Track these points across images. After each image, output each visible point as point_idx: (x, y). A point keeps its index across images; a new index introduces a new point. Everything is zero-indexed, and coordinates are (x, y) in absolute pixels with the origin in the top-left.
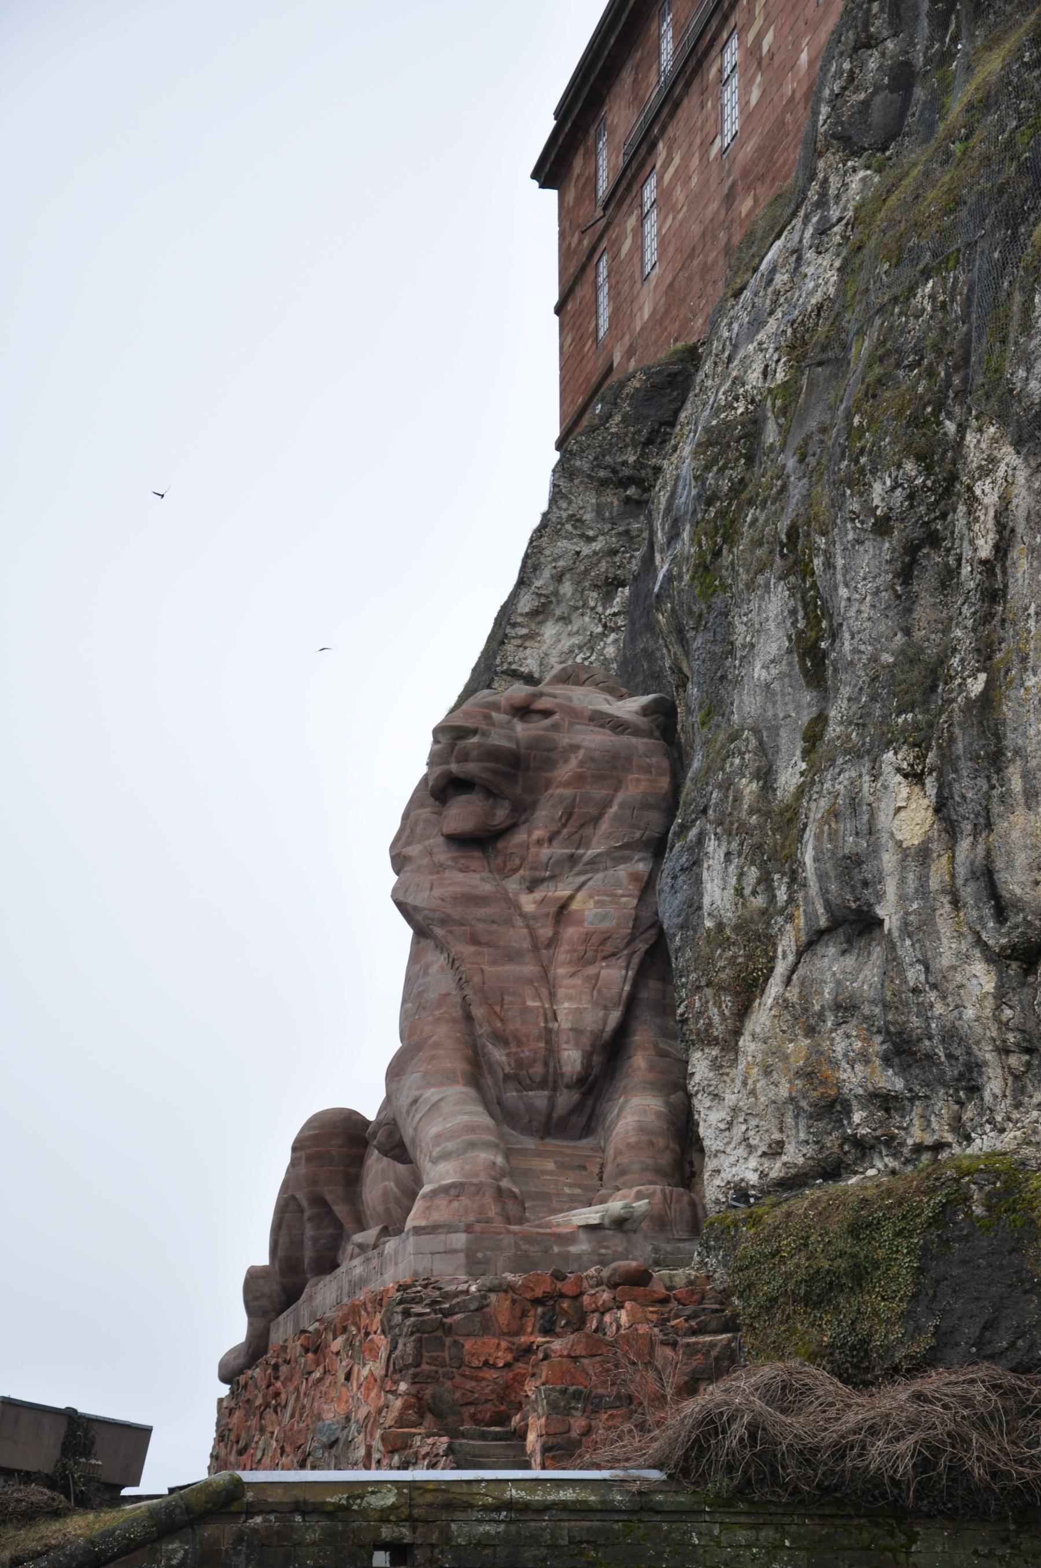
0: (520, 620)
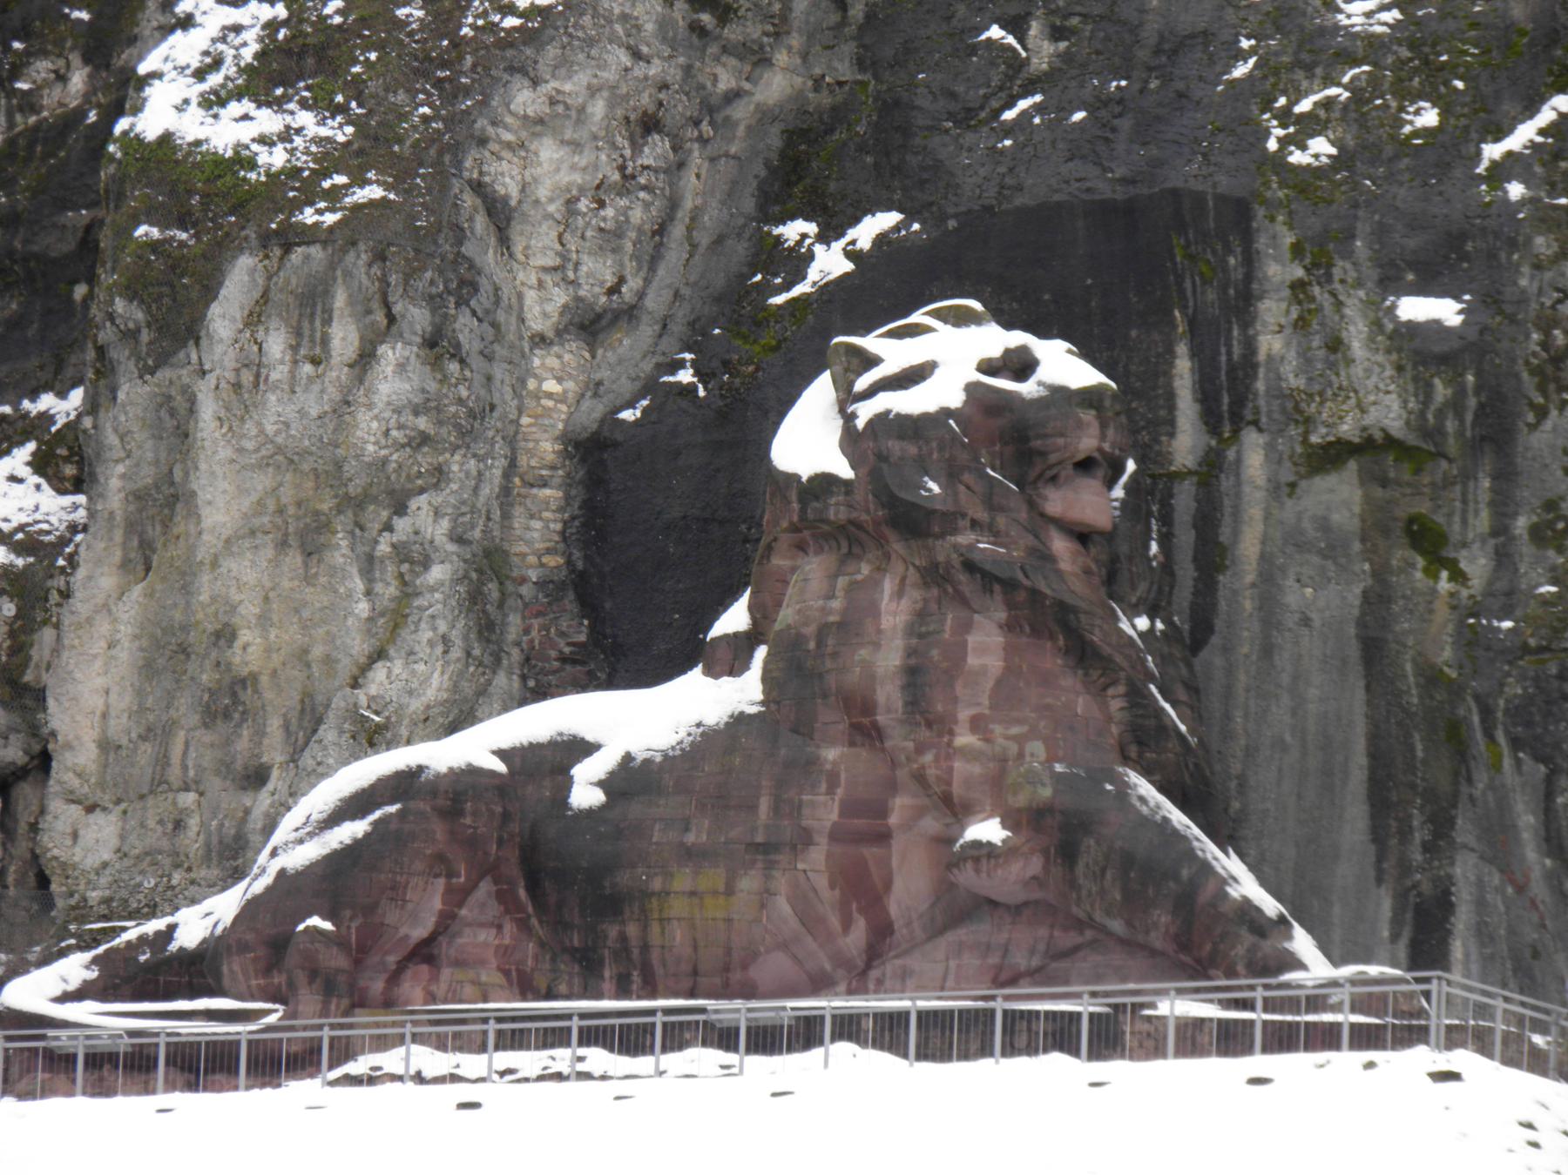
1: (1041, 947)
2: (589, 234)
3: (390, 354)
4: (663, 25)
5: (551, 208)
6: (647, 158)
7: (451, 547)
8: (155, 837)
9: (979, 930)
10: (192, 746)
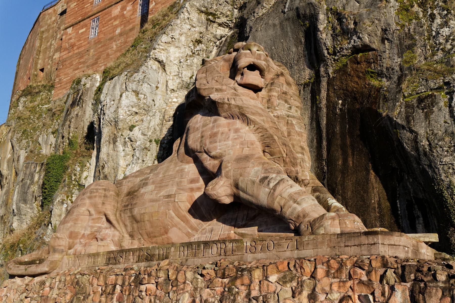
0: (161, 44)
1: (245, 218)
2: (184, 66)
4: (198, 20)
5: (175, 62)
6: (198, 48)
7: (142, 137)
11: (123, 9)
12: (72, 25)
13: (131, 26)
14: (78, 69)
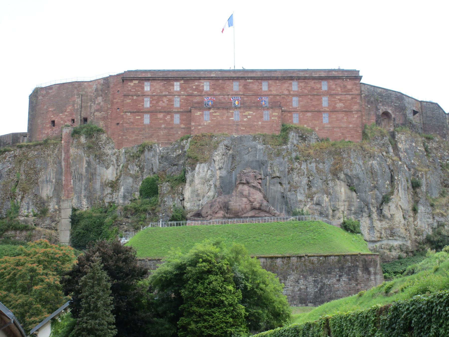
3: (209, 171)
8: (193, 204)
9: (254, 211)
10: (195, 198)
11: (165, 116)
12: (131, 112)
13: (171, 126)
14: (139, 136)
